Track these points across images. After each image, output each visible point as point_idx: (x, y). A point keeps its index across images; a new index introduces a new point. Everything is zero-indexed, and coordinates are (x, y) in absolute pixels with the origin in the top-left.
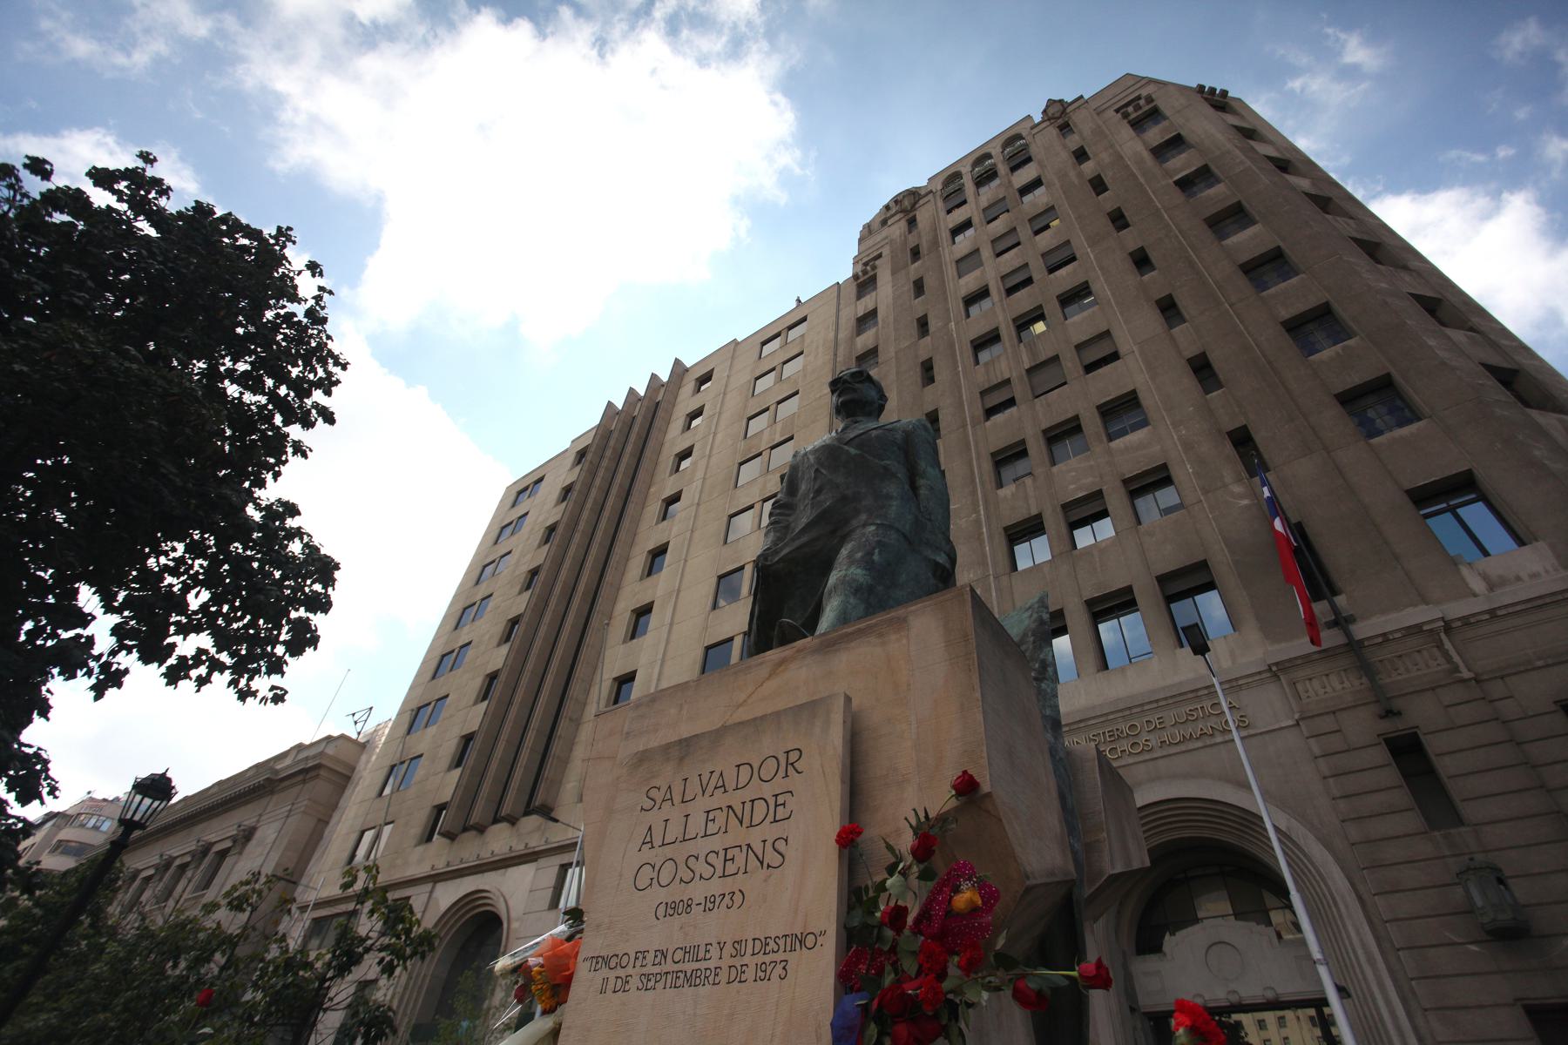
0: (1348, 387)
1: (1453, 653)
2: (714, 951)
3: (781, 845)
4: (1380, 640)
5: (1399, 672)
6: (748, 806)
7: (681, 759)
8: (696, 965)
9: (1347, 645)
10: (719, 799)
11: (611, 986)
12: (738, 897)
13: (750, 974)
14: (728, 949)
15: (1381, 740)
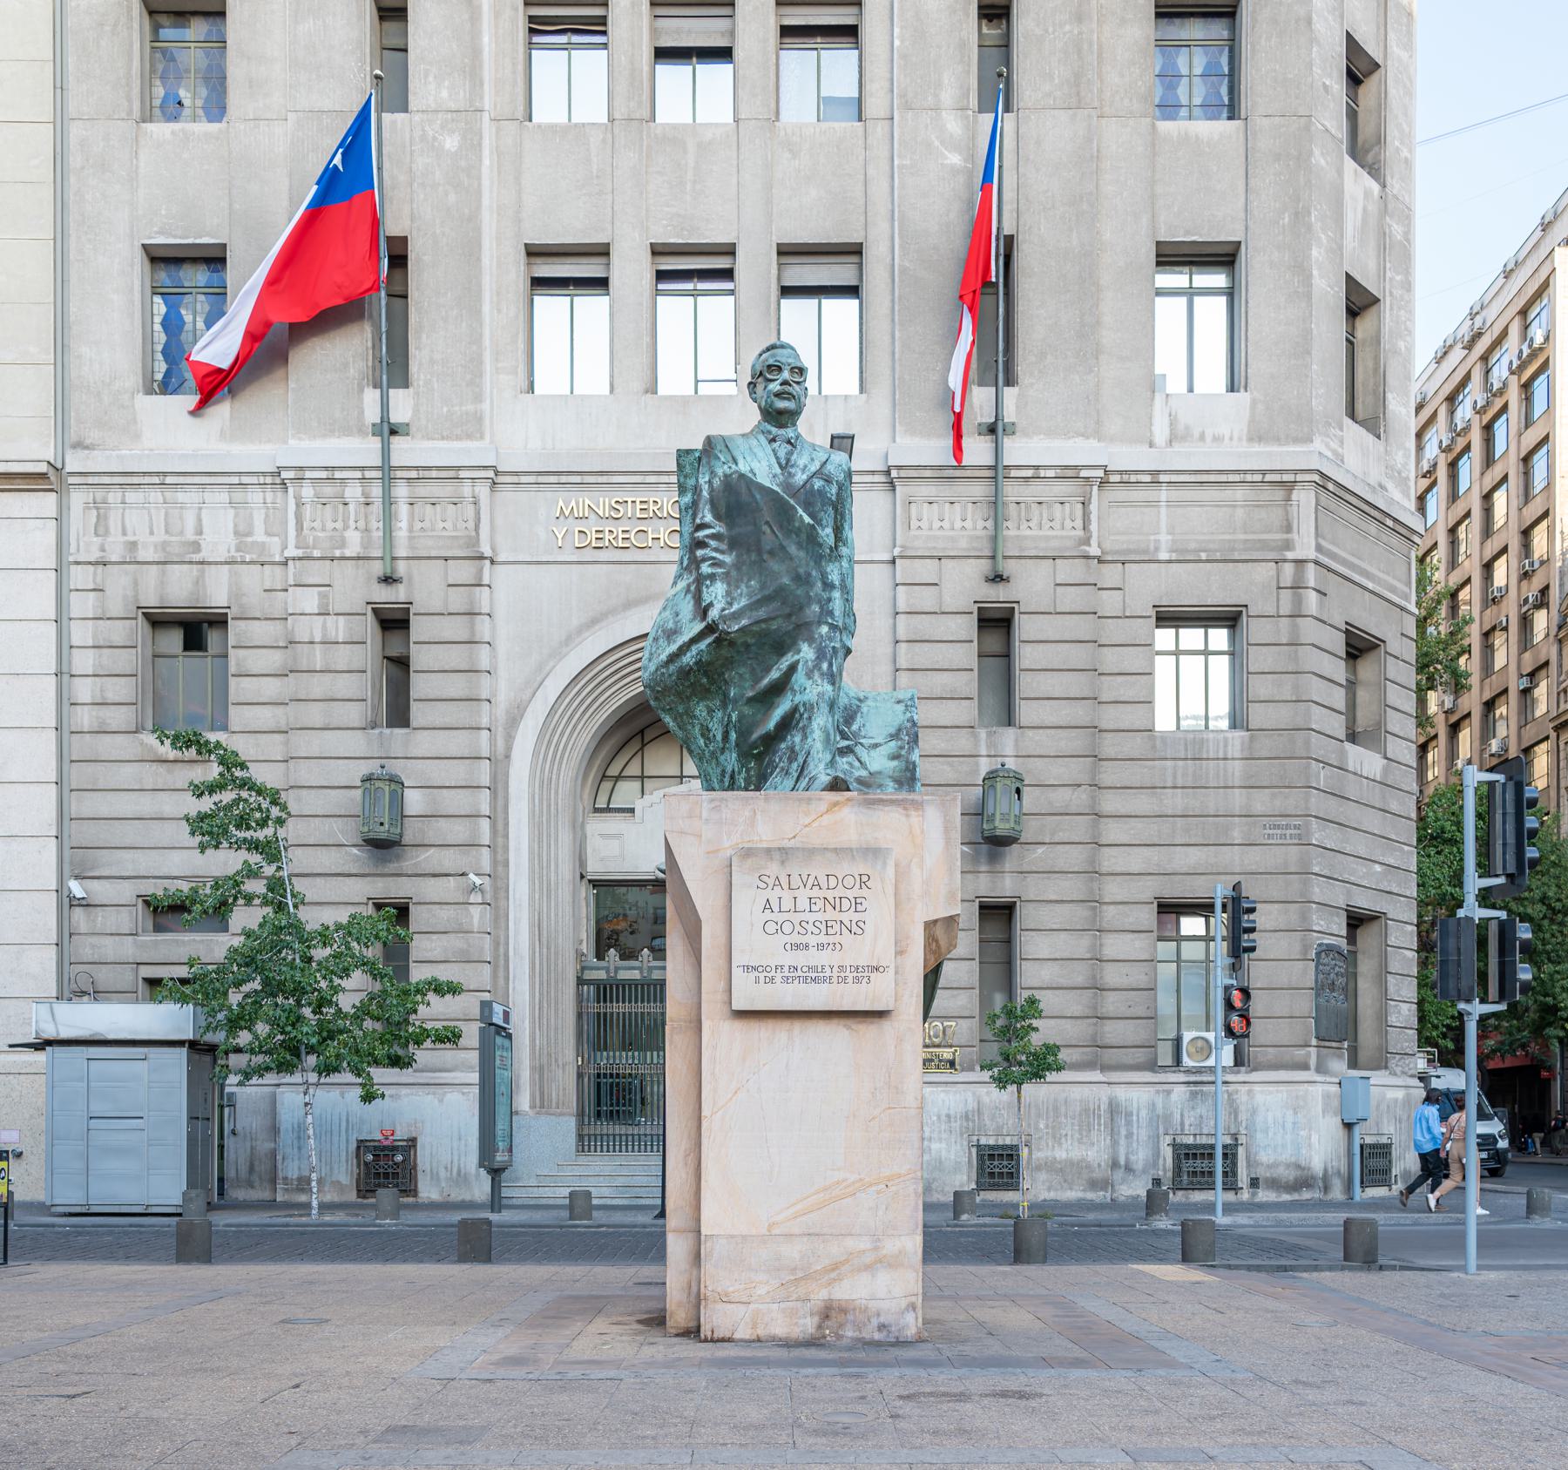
1: (1094, 518)
2: (827, 969)
5: (1031, 524)
6: (838, 900)
7: (783, 862)
10: (816, 892)
12: (838, 947)
13: (850, 980)
15: (975, 608)
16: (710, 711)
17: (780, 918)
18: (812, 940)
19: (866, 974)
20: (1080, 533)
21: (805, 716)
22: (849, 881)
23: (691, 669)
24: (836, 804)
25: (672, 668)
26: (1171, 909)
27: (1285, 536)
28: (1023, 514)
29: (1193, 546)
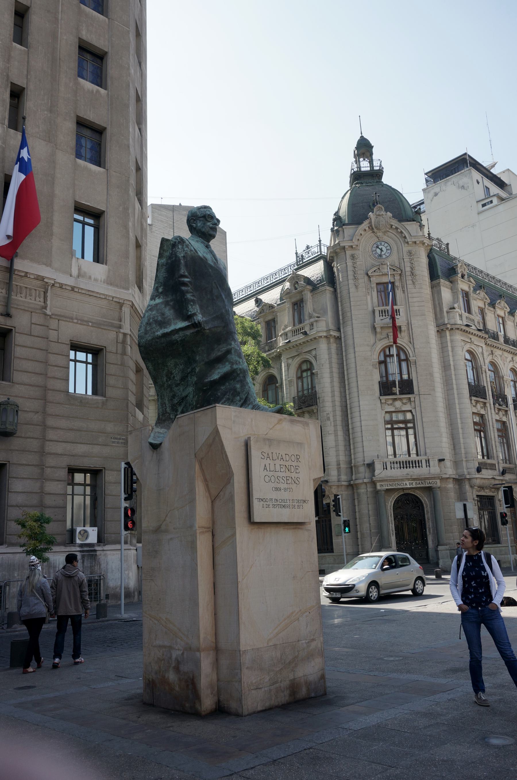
0: (85, 117)
2: (288, 501)
3: (298, 479)
4: (23, 274)
6: (290, 466)
8: (285, 504)
9: (7, 268)
10: (282, 462)
11: (265, 505)
13: (296, 507)
14: (291, 501)
16: (176, 365)
17: (271, 473)
18: (282, 486)
19: (301, 504)
20: (43, 304)
21: (241, 375)
22: (293, 458)
24: (281, 420)
25: (163, 340)
26: (72, 471)
27: (120, 323)
28: (19, 290)
29: (86, 319)
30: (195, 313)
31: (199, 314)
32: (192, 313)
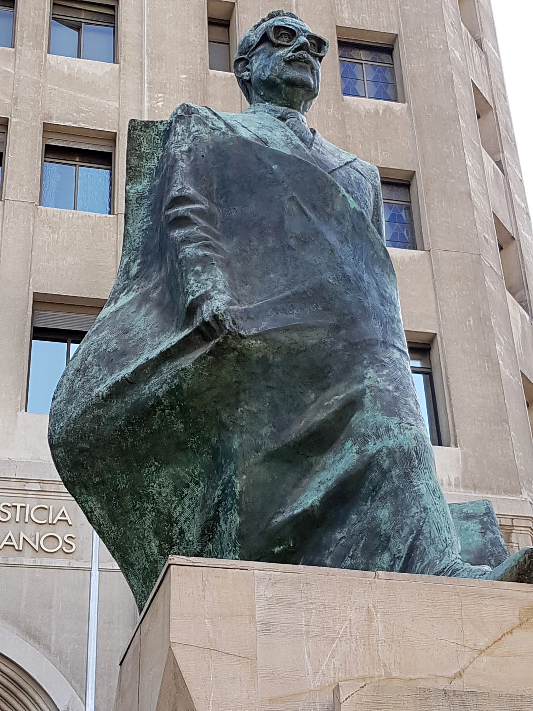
23: (159, 401)
25: (116, 407)
30: (206, 292)
31: (220, 292)
32: (198, 294)
